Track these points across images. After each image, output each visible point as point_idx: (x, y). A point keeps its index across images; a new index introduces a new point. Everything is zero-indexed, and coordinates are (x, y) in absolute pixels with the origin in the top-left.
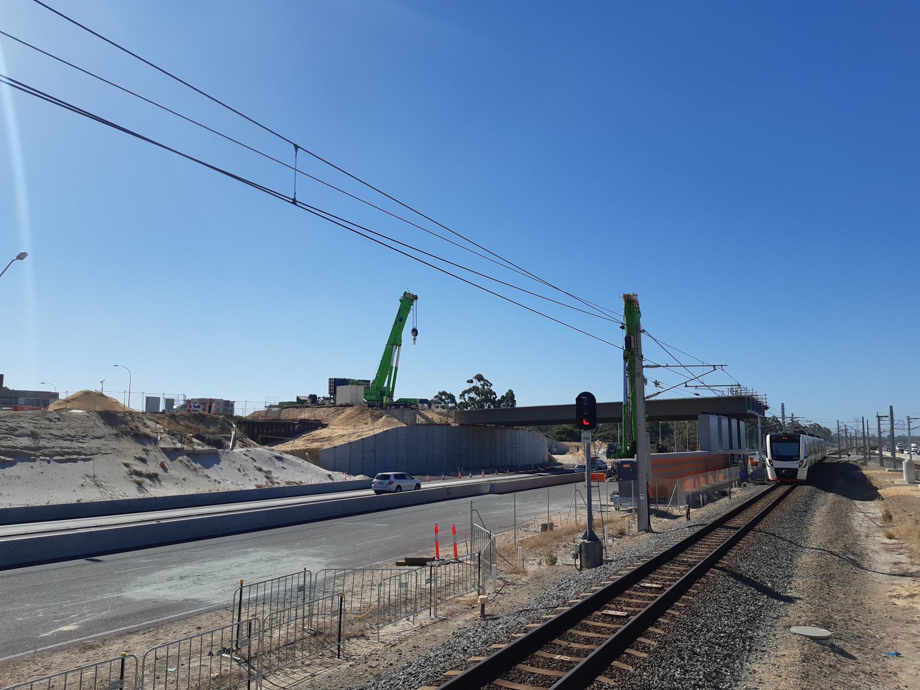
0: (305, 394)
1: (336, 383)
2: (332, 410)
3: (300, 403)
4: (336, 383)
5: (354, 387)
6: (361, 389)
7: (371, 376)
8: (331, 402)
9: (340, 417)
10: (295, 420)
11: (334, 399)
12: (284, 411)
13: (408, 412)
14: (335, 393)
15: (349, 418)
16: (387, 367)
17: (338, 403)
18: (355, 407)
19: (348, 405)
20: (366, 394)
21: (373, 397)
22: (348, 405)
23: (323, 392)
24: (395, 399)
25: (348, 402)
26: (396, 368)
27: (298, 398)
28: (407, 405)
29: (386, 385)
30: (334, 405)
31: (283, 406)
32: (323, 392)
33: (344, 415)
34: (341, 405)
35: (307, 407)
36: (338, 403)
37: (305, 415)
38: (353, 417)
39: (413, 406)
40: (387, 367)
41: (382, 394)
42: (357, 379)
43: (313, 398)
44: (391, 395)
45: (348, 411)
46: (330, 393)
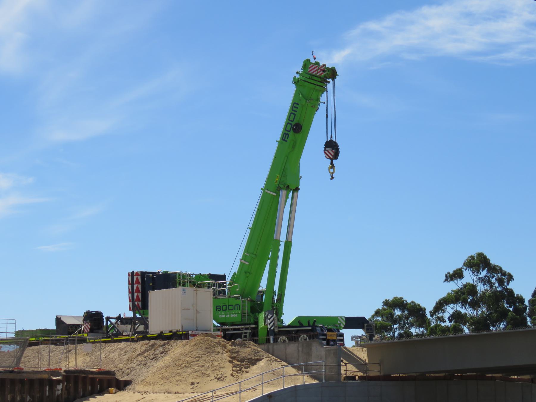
0: (74, 314)
1: (145, 284)
2: (139, 346)
3: (65, 333)
4: (145, 284)
5: (190, 290)
6: (205, 297)
7: (227, 262)
8: (136, 327)
9: (159, 364)
10: (56, 372)
11: (144, 322)
12: (30, 351)
13: (319, 350)
14: (145, 306)
15: (182, 365)
16: (265, 241)
17: (154, 329)
18: (193, 341)
19: (175, 336)
20: (218, 308)
21: (235, 316)
22: (175, 336)
23: (116, 304)
24: (288, 319)
25: (176, 327)
26: (288, 245)
27: (59, 321)
28: (317, 332)
29: (263, 285)
30: (144, 336)
31: (27, 340)
32: (116, 304)
33: (167, 359)
34: (160, 336)
35: (83, 341)
36: (154, 329)
37: (79, 359)
38: (188, 365)
39: (331, 336)
40: (265, 241)
41: (256, 308)
42: (195, 271)
43: (94, 319)
44: (276, 309)
45: (178, 348)
46: (133, 308)
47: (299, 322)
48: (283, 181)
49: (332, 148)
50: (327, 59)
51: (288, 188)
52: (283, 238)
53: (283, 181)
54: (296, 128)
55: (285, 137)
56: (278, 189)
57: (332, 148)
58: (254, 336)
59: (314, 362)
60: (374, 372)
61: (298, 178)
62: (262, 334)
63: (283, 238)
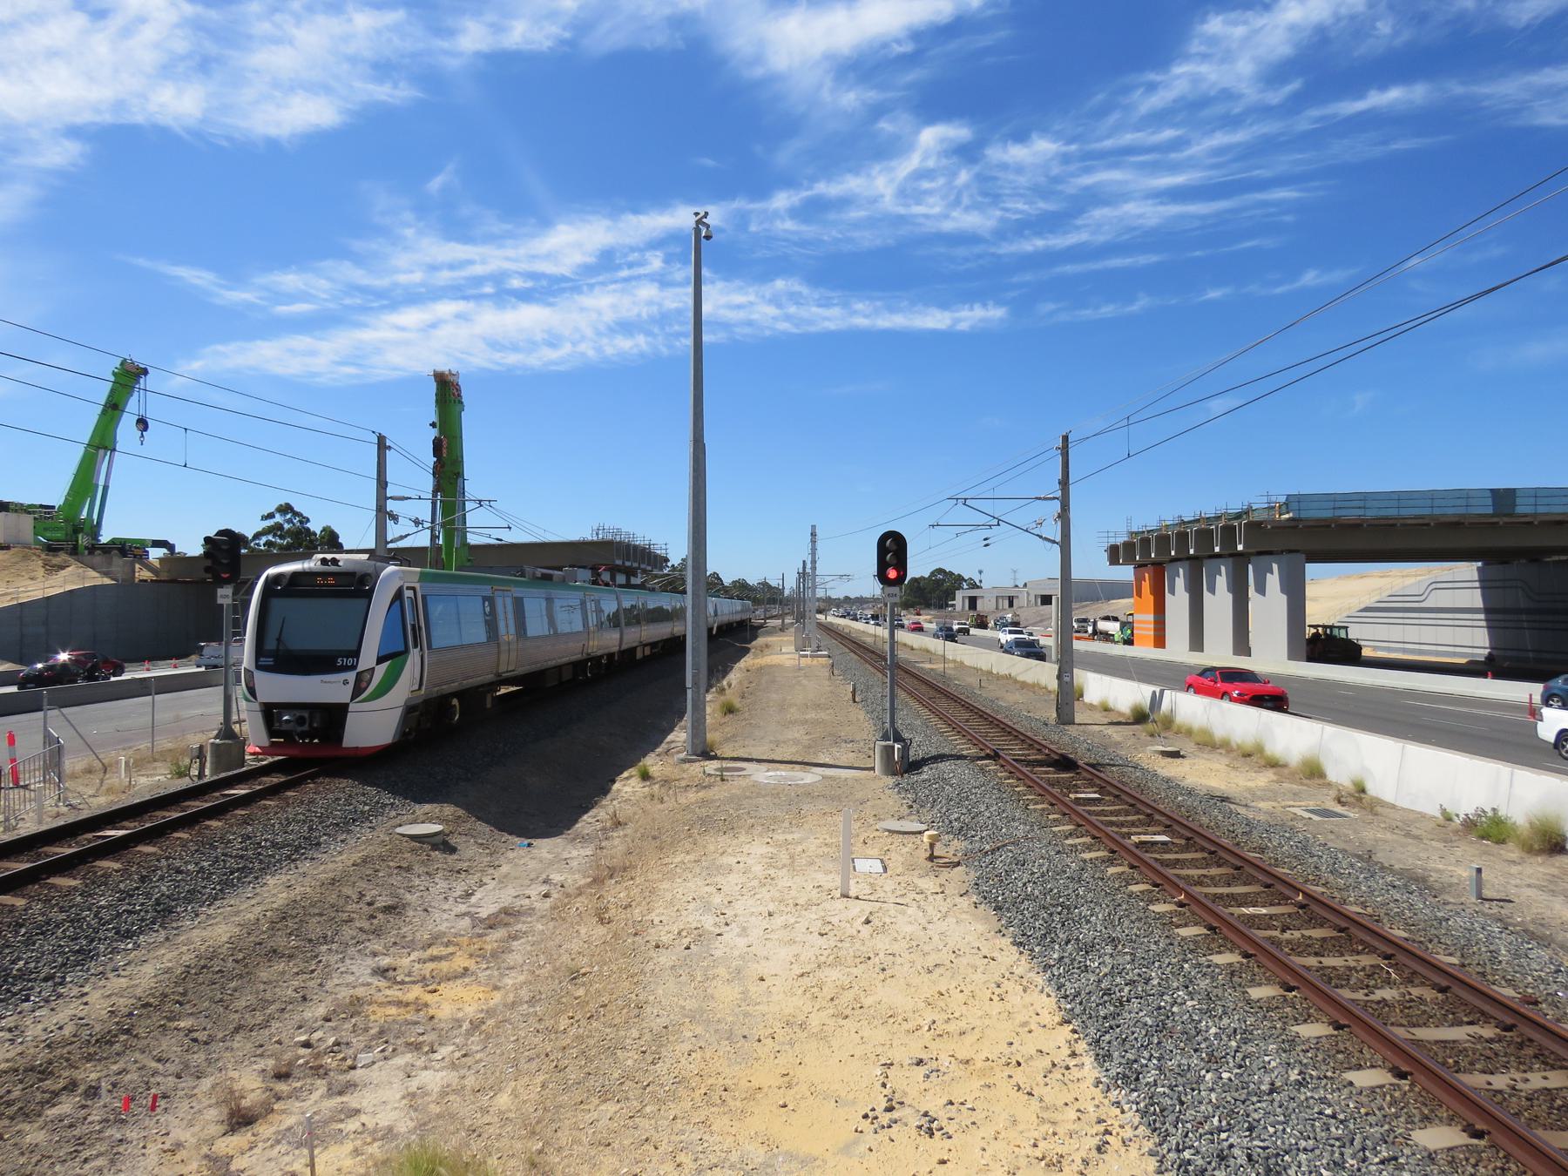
6: (27, 522)
16: (85, 483)
24: (105, 538)
26: (106, 488)
28: (128, 550)
39: (137, 552)
47: (113, 541)
48: (102, 443)
49: (143, 424)
50: (141, 359)
51: (106, 448)
52: (101, 482)
53: (102, 443)
54: (113, 408)
55: (104, 412)
56: (98, 448)
57: (143, 424)
58: (74, 551)
59: (113, 569)
60: (164, 576)
61: (115, 441)
62: (81, 549)
63: (101, 482)
